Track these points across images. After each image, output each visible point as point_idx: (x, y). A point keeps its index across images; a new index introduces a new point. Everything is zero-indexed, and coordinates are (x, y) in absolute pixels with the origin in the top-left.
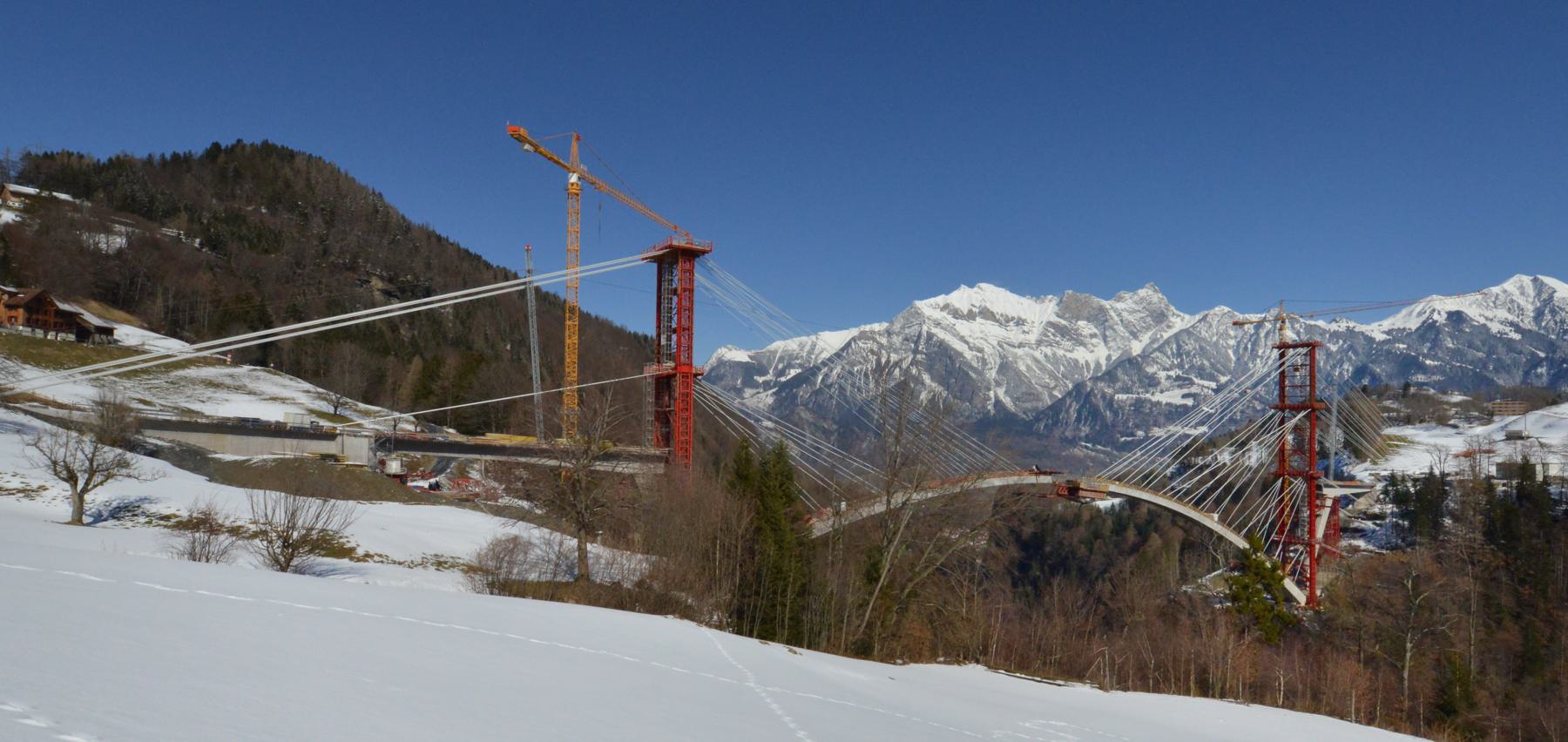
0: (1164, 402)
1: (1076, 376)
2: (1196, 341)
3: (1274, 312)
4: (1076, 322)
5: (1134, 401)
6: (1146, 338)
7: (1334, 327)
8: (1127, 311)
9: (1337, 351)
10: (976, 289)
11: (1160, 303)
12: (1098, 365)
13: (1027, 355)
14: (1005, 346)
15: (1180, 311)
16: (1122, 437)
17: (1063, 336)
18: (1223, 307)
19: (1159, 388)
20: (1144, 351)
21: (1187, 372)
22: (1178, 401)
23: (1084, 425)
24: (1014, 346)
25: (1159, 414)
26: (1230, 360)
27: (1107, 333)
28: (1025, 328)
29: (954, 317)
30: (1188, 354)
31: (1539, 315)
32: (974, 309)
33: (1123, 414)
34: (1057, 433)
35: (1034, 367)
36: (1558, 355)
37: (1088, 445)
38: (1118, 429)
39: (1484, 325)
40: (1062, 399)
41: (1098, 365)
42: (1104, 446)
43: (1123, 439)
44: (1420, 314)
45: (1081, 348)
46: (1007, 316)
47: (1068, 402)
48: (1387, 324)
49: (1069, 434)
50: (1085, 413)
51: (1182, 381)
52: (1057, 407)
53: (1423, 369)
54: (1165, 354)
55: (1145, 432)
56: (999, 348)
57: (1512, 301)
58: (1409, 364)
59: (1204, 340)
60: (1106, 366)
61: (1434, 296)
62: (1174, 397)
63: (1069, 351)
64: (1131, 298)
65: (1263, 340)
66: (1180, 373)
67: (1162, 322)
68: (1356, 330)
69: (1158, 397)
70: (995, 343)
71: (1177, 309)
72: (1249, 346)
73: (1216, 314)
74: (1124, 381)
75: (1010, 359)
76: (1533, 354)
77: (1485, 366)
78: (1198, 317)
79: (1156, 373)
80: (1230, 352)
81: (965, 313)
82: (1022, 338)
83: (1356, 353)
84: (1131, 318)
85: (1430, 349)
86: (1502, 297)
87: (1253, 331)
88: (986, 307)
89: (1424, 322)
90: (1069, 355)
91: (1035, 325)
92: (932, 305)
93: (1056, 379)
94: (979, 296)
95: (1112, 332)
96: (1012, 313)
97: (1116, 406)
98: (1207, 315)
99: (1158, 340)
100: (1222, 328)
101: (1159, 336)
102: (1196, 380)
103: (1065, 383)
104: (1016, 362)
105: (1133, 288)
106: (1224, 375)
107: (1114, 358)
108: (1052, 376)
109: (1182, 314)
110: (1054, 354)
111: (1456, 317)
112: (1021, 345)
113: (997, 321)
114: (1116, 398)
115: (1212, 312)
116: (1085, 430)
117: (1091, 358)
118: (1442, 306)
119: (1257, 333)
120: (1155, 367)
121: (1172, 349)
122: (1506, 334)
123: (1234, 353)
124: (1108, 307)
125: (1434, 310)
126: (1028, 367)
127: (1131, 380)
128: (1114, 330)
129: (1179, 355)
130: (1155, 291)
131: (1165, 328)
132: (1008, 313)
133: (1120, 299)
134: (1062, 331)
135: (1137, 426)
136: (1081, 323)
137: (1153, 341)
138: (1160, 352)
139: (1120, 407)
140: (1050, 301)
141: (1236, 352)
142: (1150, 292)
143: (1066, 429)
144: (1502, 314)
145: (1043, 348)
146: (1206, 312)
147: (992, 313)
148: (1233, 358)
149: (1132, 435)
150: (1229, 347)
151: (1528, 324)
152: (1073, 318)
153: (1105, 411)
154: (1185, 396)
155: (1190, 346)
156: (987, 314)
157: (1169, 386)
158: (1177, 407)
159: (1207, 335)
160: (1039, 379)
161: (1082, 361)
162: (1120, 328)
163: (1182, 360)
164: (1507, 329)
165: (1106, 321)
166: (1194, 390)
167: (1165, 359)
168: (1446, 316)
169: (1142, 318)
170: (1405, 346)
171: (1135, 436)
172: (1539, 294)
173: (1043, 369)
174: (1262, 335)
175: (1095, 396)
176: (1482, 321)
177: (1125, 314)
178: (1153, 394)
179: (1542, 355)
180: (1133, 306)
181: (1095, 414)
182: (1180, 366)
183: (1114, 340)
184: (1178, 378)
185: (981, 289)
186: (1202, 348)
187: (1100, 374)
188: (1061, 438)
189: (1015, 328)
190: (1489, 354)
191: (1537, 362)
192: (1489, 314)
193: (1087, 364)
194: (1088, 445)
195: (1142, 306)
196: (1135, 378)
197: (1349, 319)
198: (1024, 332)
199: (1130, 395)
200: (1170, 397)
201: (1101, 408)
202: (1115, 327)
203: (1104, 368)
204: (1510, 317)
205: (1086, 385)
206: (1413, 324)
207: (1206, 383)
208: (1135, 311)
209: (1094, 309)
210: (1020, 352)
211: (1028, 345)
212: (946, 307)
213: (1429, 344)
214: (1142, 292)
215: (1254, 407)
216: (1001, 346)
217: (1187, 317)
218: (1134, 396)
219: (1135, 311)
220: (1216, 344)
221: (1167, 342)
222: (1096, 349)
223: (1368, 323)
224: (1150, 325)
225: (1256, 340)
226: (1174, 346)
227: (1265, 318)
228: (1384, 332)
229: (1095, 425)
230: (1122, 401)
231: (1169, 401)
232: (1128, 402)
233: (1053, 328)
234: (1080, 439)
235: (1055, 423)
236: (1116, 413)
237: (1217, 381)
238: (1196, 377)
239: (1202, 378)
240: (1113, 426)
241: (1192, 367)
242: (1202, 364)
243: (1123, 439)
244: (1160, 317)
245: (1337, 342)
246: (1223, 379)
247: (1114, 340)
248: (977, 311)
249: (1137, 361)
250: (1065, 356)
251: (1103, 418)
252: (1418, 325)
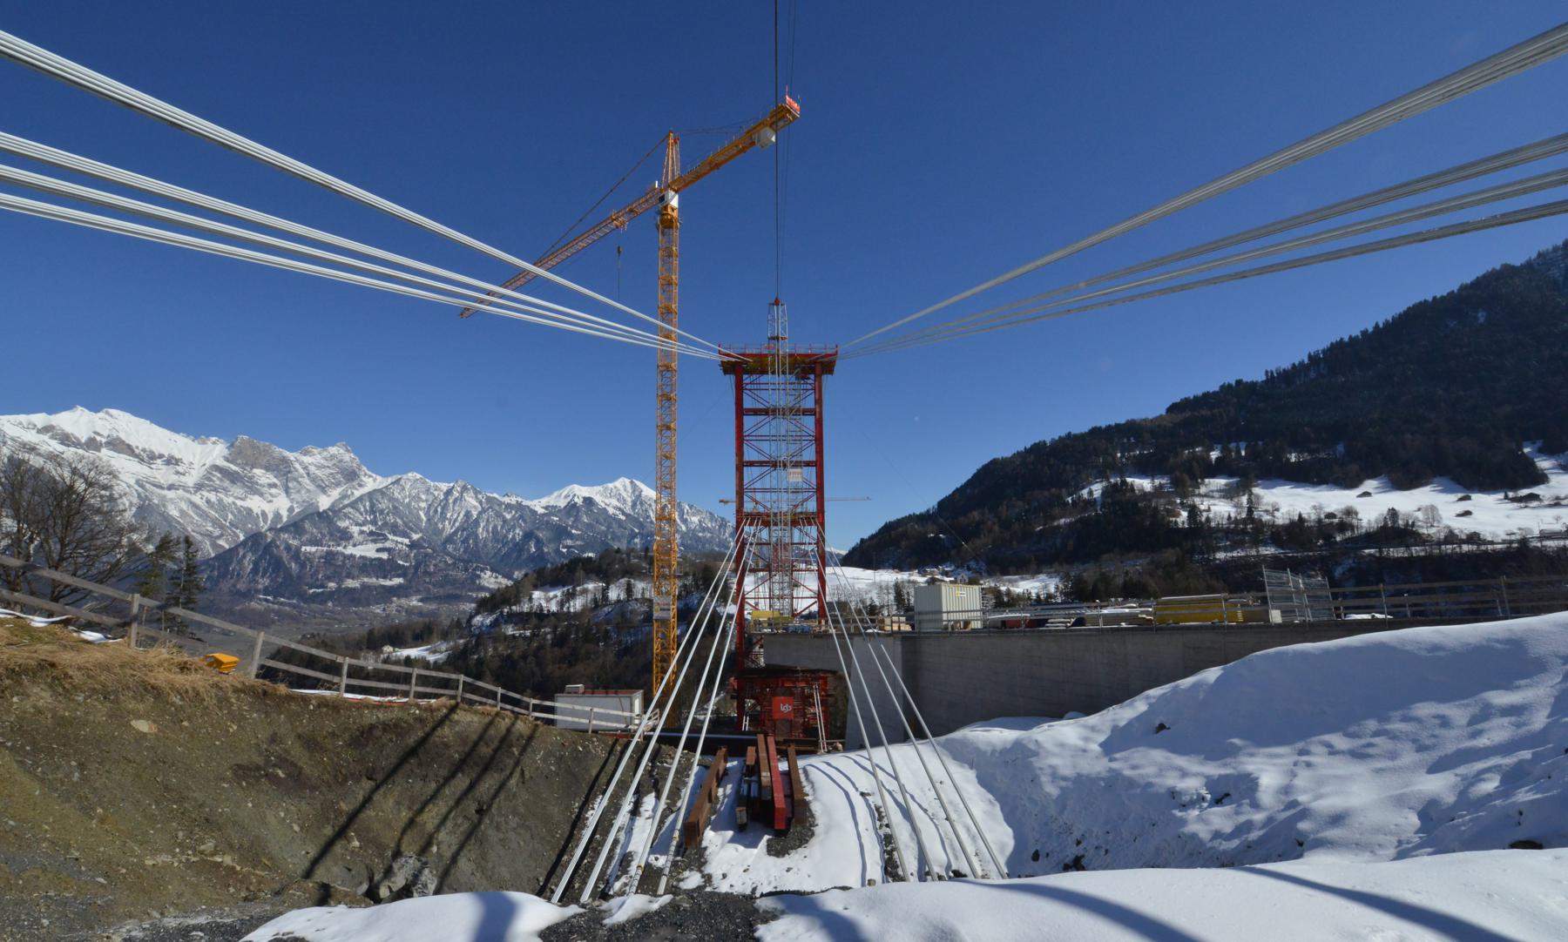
0: (358, 555)
1: (250, 526)
2: (389, 501)
3: (461, 483)
4: (251, 469)
5: (323, 554)
6: (335, 493)
7: (507, 500)
8: (315, 466)
9: (511, 519)
10: (101, 415)
11: (352, 462)
12: (278, 516)
13: (181, 499)
14: (147, 486)
15: (373, 472)
16: (310, 588)
17: (233, 482)
18: (415, 473)
19: (351, 542)
20: (333, 505)
21: (380, 528)
22: (373, 555)
23: (263, 577)
24: (163, 488)
25: (352, 566)
26: (422, 520)
27: (290, 485)
28: (180, 469)
29: (62, 443)
30: (382, 512)
31: (634, 505)
32: (98, 438)
33: (311, 566)
34: (225, 586)
35: (192, 513)
36: (645, 532)
37: (268, 598)
38: (306, 581)
39: (605, 509)
40: (230, 550)
41: (278, 516)
42: (289, 599)
43: (312, 590)
44: (566, 497)
45: (256, 498)
46: (152, 452)
47: (241, 554)
48: (545, 501)
49: (241, 586)
50: (264, 564)
51: (375, 536)
52: (225, 558)
53: (570, 536)
54: (358, 510)
55: (337, 583)
56: (137, 487)
57: (620, 494)
58: (561, 532)
59: (397, 500)
60: (288, 516)
61: (575, 485)
62: (369, 551)
63: (241, 499)
64: (320, 453)
65: (451, 505)
66: (374, 529)
67: (353, 480)
68: (523, 504)
69: (350, 550)
70: (132, 482)
71: (368, 469)
72: (439, 509)
73: (408, 479)
74: (312, 534)
75: (156, 501)
76: (632, 530)
77: (606, 536)
78: (390, 480)
79: (348, 528)
80: (421, 513)
81: (83, 441)
82: (173, 479)
83: (524, 521)
84: (318, 473)
85: (574, 522)
86: (614, 490)
87: (442, 497)
88: (118, 438)
89: (569, 503)
90: (239, 503)
91: (193, 466)
92: (21, 423)
93: (222, 527)
94: (107, 424)
95: (295, 483)
96: (157, 450)
97: (303, 558)
98: (400, 479)
99: (349, 497)
100: (414, 492)
101: (349, 493)
102: (390, 537)
103: (234, 532)
104: (164, 506)
105: (324, 445)
106: (416, 533)
107: (297, 510)
108: (215, 522)
109: (374, 475)
110: (220, 501)
111: (589, 501)
112: (171, 487)
113: (137, 456)
114: (303, 549)
115: (405, 477)
116: (264, 582)
117: (269, 509)
118: (581, 492)
119: (446, 499)
120: (347, 522)
121: (364, 506)
123: (425, 515)
124: (292, 458)
125: (575, 495)
126: (182, 512)
127: (321, 533)
128: (298, 482)
129: (372, 511)
130: (347, 451)
131: (357, 487)
132: (153, 449)
133: (306, 453)
134: (233, 478)
135: (329, 579)
136: (257, 471)
137: (344, 497)
138: (353, 508)
139: (309, 559)
140: (214, 443)
141: (427, 514)
142: (342, 451)
143: (237, 581)
144: (614, 502)
145: (205, 494)
146: (399, 476)
147: (129, 446)
148: (424, 519)
149: (322, 586)
150: (420, 509)
151: (628, 510)
152: (247, 464)
153: (289, 563)
154: (378, 550)
155: (384, 504)
156: (118, 445)
157: (362, 540)
158: (372, 560)
159: (400, 497)
160: (198, 526)
161: (256, 510)
162: (306, 481)
163: (375, 517)
164: (618, 512)
165: (290, 472)
166: (388, 545)
167: (357, 515)
168: (582, 500)
169: (332, 474)
171: (327, 587)
172: (634, 491)
173: (204, 515)
174: (451, 501)
175: (278, 547)
176: (603, 505)
177: (312, 469)
178: (345, 547)
179: (637, 531)
180: (322, 461)
181: (277, 565)
182: (374, 522)
183: (299, 492)
184: (372, 533)
185: (111, 416)
186: (395, 508)
187: (279, 526)
188: (231, 591)
189: (164, 467)
190: (609, 527)
191: (634, 536)
192: (607, 501)
193: (264, 513)
194: (268, 598)
195: (333, 462)
196: (325, 531)
197: (517, 495)
198: (178, 473)
199: (320, 548)
200: (363, 551)
201: (285, 559)
202: (300, 479)
203: (285, 519)
204: (619, 505)
205: (266, 536)
206: (562, 504)
207: (400, 539)
208: (324, 467)
209: (274, 458)
210: (170, 494)
211: (185, 488)
212: (47, 429)
213: (572, 519)
214: (333, 450)
215: (446, 562)
216: (142, 486)
217: (379, 478)
218: (325, 549)
219: (324, 467)
220: (409, 505)
221: (361, 499)
222: (274, 499)
223: (532, 500)
224: (340, 481)
225: (445, 504)
226: (368, 504)
227: (453, 487)
228: (543, 508)
229: (276, 577)
230: (310, 553)
231: (363, 554)
232: (318, 555)
233: (220, 473)
234: (257, 591)
235: (224, 575)
236: (303, 565)
237: (409, 537)
238: (390, 533)
239: (395, 534)
240: (299, 577)
241: (385, 524)
242: (395, 521)
243: (312, 590)
244: (351, 476)
245: (511, 512)
246: (415, 537)
247: (299, 492)
248: (104, 440)
249: (328, 515)
250: (234, 503)
251: (288, 570)
252: (565, 504)
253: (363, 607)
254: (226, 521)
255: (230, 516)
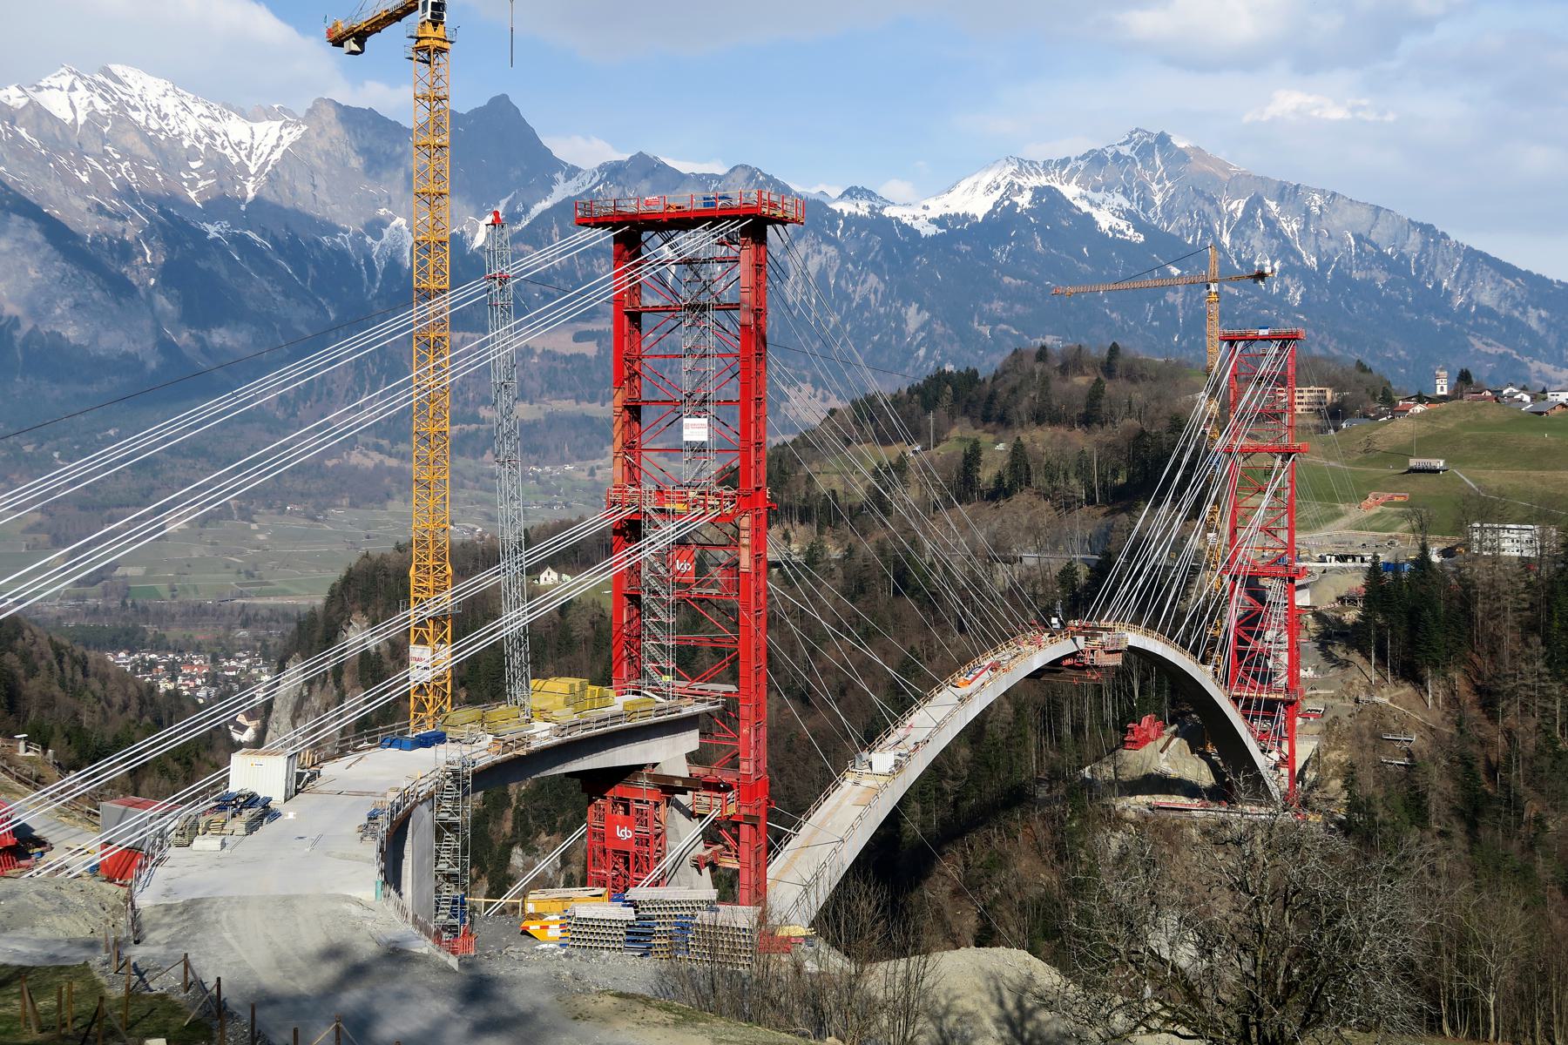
39: (1089, 215)
89: (996, 205)
122: (1121, 232)
151: (1155, 217)
154: (579, 338)
158: (568, 359)
164: (1123, 225)
170: (969, 248)
176: (1085, 207)
204: (1126, 205)
228: (933, 221)
253: (554, 464)
254: (304, 279)
255: (311, 271)
